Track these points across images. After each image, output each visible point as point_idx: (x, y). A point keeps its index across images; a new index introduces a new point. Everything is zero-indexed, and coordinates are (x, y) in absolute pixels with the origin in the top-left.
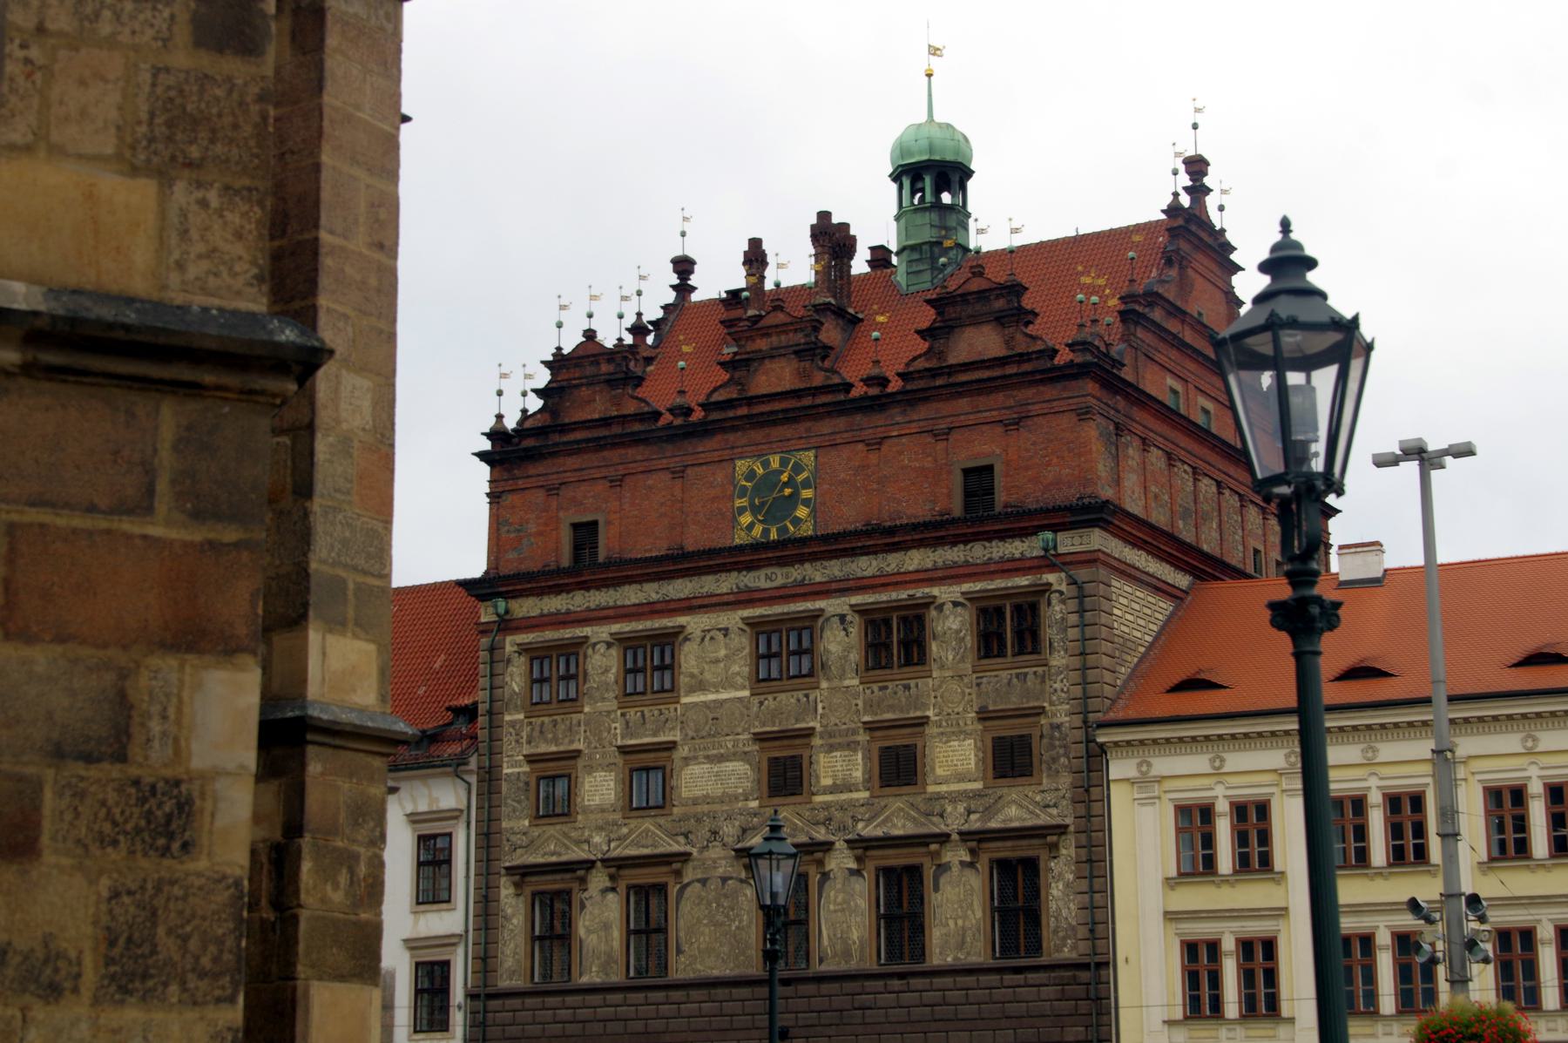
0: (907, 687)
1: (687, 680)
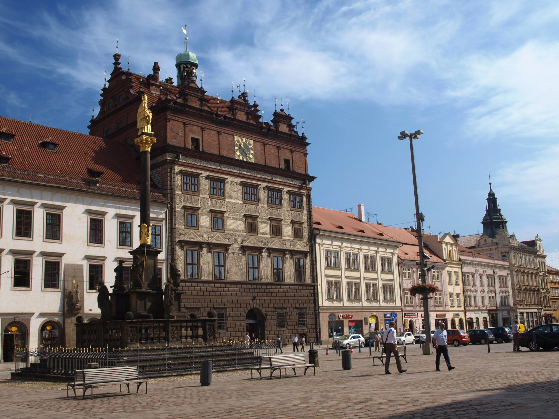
0: (277, 210)
1: (227, 194)
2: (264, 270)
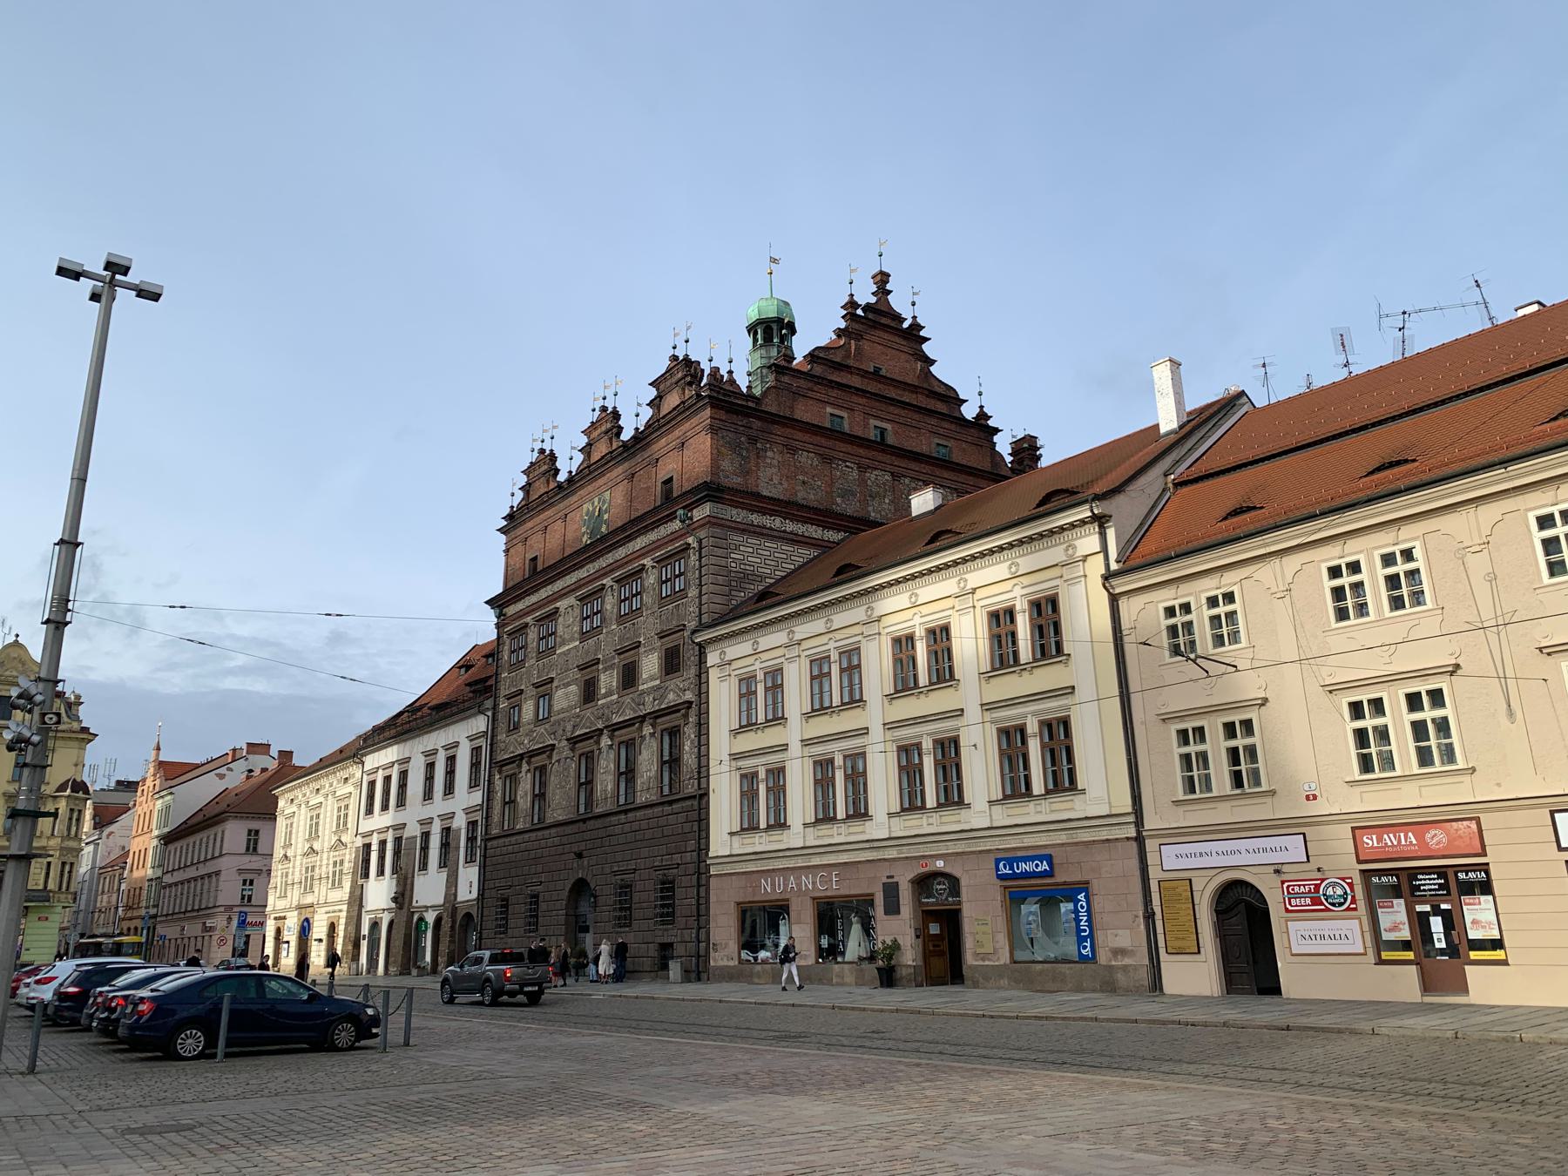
2: (601, 784)
